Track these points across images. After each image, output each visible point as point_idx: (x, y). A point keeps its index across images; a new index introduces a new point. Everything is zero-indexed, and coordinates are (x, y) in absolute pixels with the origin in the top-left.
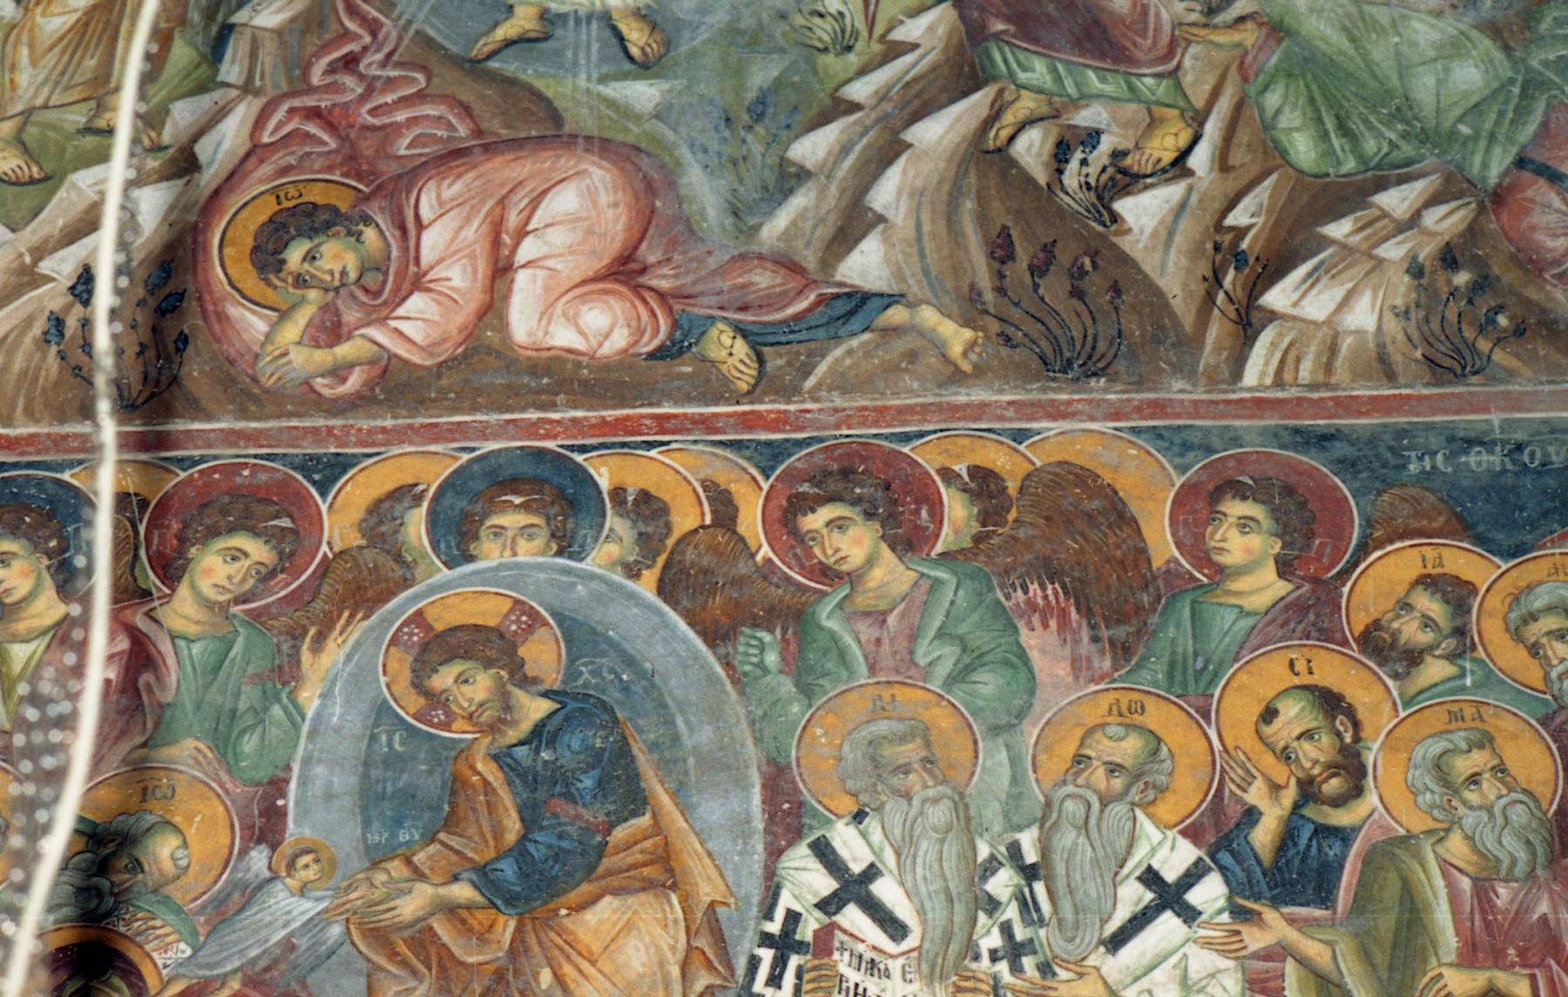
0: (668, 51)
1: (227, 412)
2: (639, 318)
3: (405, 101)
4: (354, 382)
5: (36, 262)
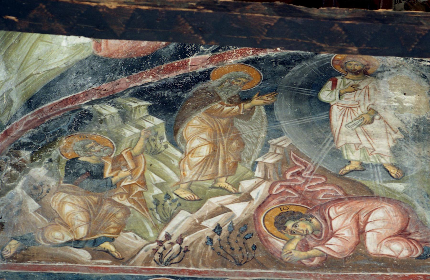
0: (404, 176)
1: (273, 268)
2: (411, 247)
3: (318, 185)
4: (316, 261)
5: (201, 222)
